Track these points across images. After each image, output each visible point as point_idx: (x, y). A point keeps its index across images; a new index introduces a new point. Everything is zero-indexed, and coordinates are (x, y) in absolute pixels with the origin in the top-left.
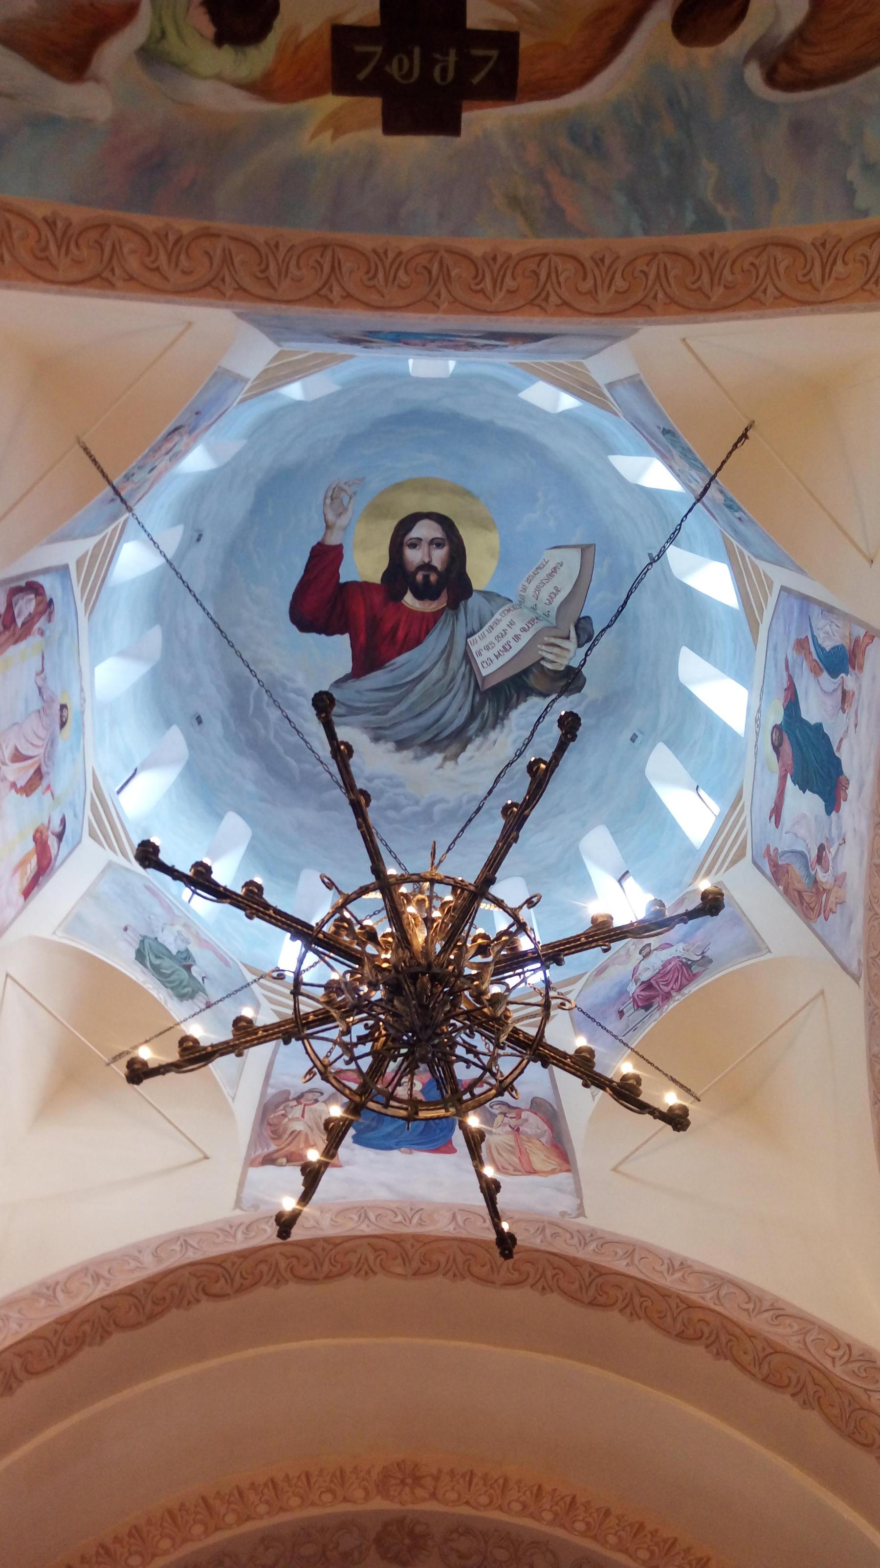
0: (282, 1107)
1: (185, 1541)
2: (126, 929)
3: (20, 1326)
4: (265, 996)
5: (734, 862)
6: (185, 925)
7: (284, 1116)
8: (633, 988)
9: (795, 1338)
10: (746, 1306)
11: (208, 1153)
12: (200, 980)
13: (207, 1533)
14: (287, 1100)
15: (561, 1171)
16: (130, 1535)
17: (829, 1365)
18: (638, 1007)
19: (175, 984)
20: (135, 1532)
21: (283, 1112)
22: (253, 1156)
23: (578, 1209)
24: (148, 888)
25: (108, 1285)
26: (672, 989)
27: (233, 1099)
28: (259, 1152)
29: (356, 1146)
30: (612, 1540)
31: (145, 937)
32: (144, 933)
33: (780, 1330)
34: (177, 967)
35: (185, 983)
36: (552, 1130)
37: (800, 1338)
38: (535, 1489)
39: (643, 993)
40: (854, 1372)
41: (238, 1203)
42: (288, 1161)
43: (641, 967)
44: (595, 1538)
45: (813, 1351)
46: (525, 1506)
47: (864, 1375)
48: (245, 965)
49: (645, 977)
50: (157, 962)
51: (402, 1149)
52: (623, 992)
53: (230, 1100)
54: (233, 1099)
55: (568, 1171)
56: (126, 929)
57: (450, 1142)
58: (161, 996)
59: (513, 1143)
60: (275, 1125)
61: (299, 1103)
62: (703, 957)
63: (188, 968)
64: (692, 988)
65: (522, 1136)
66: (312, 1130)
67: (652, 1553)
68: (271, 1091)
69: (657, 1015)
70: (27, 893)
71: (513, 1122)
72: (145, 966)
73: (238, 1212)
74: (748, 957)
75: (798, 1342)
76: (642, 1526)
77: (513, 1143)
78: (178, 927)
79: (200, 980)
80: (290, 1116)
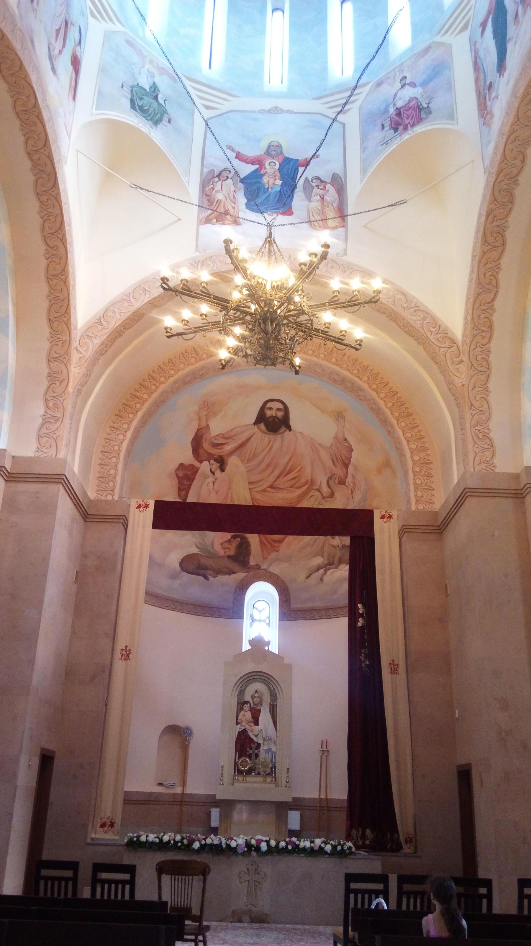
0: (211, 183)
1: (189, 365)
2: (122, 87)
3: (120, 315)
4: (198, 96)
5: (461, 31)
6: (151, 62)
7: (213, 188)
8: (392, 110)
9: (419, 322)
10: (404, 305)
11: (181, 218)
12: (163, 104)
13: (196, 362)
14: (214, 177)
15: (340, 227)
16: (169, 362)
17: (429, 335)
18: (392, 127)
19: (152, 115)
20: (170, 361)
21: (212, 186)
22: (201, 217)
23: (345, 251)
24: (127, 42)
25: (150, 294)
26: (409, 123)
27: (188, 183)
28: (203, 215)
29: (247, 211)
30: (345, 366)
31: (132, 87)
32: (131, 85)
33: (414, 318)
34: (151, 100)
35: (156, 112)
36: (339, 197)
37: (421, 322)
38: (318, 345)
39: (395, 117)
40: (438, 339)
41: (197, 250)
42: (217, 221)
43: (399, 95)
44: (338, 365)
45: (425, 329)
46: (314, 351)
47: (441, 340)
48: (185, 76)
49: (400, 104)
50: (140, 103)
51: (269, 212)
52: (386, 111)
53: (187, 184)
54: (188, 183)
55: (343, 226)
56: (122, 87)
57: (291, 207)
58: (147, 129)
59: (320, 208)
60: (209, 196)
61: (220, 179)
62: (428, 107)
63: (156, 98)
64: (419, 129)
65: (325, 203)
66: (226, 200)
67: (358, 371)
68: (206, 170)
69: (398, 140)
70: (74, 98)
71: (321, 192)
72: (136, 110)
73: (197, 254)
74: (448, 122)
75: (420, 324)
76: (356, 360)
77: (320, 208)
78: (148, 66)
79: (163, 104)
80: (216, 189)
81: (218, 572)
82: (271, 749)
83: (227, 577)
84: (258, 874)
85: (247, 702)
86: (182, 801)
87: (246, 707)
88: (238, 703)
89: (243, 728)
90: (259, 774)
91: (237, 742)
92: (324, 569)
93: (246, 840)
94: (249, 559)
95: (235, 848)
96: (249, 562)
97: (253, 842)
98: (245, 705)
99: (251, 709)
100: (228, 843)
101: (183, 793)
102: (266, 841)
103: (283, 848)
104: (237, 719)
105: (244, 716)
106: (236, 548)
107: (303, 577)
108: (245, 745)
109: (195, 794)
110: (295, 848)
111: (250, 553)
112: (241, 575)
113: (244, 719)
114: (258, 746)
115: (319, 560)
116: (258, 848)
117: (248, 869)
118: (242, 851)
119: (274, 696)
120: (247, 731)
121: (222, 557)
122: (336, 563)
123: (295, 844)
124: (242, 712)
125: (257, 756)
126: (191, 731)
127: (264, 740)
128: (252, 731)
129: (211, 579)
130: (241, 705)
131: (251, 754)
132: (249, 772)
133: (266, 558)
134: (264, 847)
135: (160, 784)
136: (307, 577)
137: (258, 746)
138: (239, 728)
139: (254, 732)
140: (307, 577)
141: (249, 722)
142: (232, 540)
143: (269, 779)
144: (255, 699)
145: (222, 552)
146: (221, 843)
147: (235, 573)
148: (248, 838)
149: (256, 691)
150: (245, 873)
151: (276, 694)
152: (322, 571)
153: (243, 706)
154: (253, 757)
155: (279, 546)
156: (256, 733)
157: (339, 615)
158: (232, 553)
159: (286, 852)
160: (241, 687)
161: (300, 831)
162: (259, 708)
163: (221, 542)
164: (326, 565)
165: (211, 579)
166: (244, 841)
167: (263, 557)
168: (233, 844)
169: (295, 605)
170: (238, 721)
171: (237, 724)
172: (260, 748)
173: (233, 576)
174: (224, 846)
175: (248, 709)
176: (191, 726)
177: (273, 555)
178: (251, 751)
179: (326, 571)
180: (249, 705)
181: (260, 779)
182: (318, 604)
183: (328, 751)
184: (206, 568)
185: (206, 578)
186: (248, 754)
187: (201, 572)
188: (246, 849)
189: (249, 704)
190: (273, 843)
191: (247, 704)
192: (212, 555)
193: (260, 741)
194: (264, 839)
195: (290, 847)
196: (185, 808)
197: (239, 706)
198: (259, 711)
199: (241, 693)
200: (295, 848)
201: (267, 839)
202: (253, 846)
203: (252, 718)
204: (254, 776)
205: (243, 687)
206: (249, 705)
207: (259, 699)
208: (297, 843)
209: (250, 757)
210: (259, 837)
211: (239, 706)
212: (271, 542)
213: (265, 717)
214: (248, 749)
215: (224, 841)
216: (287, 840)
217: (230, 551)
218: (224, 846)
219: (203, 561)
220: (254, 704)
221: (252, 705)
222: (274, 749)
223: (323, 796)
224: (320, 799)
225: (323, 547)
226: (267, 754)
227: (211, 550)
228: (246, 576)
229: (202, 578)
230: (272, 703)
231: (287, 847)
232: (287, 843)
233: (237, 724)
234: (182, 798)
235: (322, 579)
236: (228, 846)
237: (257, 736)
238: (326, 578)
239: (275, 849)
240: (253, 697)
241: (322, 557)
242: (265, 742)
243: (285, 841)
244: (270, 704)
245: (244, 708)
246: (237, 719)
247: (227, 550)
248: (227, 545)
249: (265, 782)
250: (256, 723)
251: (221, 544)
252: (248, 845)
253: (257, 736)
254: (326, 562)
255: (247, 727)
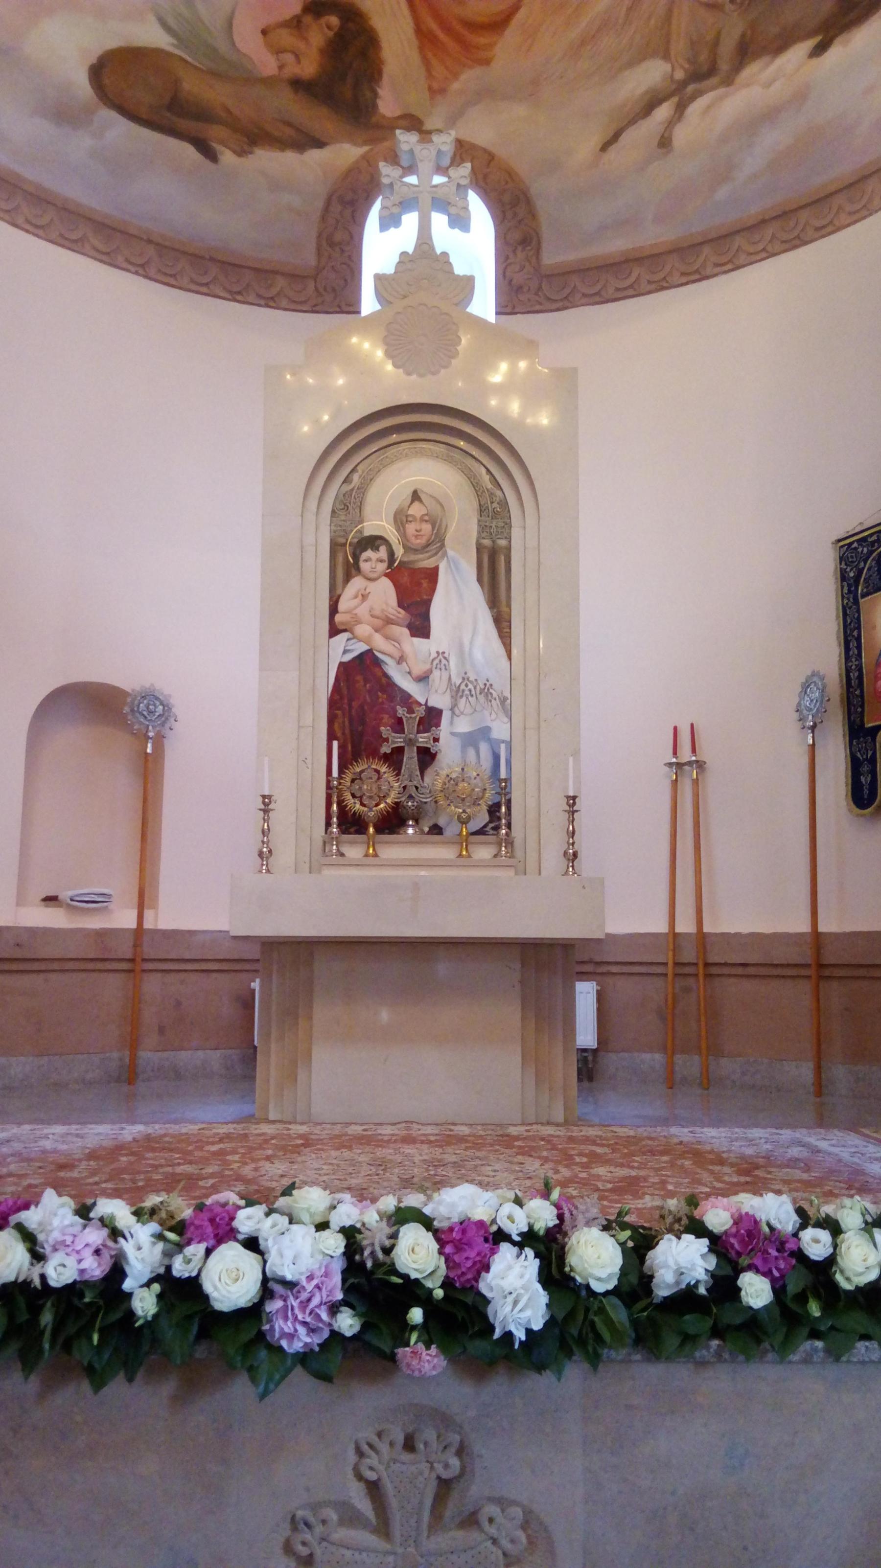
81: (253, 137)
82: (488, 729)
83: (290, 157)
84: (471, 1521)
85: (374, 542)
86: (139, 957)
87: (373, 561)
88: (335, 547)
89: (361, 648)
90: (437, 830)
91: (334, 704)
92: (675, 99)
93: (350, 1233)
94: (376, 95)
95: (252, 1313)
96: (375, 106)
97: (418, 1255)
98: (369, 553)
99: (396, 572)
100: (180, 1268)
101: (139, 931)
102: (529, 1238)
103: (685, 1299)
104: (334, 610)
105: (364, 597)
106: (322, 51)
107: (585, 147)
108: (368, 718)
109: (192, 933)
110: (802, 1298)
111: (380, 73)
112: (345, 153)
113: (363, 611)
114: (431, 718)
115: (653, 73)
116: (459, 1315)
117: (374, 1488)
118: (316, 1340)
119: (494, 515)
120: (377, 663)
121: (268, 82)
122: (724, 66)
123: (800, 1256)
124: (357, 583)
125: (427, 757)
126: (167, 707)
127: (457, 693)
128: (401, 660)
129: (227, 157)
130: (348, 555)
131: (400, 751)
132: (392, 822)
133: (442, 91)
134: (515, 1292)
135: (51, 900)
136: (605, 147)
137: (431, 718)
138: (342, 649)
139: (408, 662)
140: (605, 147)
141: (389, 621)
142: (308, 19)
143: (483, 852)
144: (411, 528)
145: (267, 64)
146: (117, 1272)
147: (320, 144)
148: (371, 1218)
149: (416, 496)
150: (350, 1517)
151: (504, 504)
152: (663, 112)
153: (356, 558)
154: (410, 759)
155: (491, 46)
156: (418, 670)
157: (742, 259)
158: (309, 68)
159: (716, 1332)
160: (347, 480)
161: (595, 1052)
162: (428, 563)
163: (261, 26)
164: (684, 83)
165: (227, 157)
166: (335, 1243)
167: (430, 88)
168: (230, 1281)
169: (554, 256)
170: (338, 618)
171: (334, 631)
172: (438, 725)
173: (314, 155)
174: (145, 1304)
175: (382, 567)
176: (165, 686)
177: (469, 78)
178: (398, 740)
179: (681, 109)
180: (383, 552)
181: (446, 853)
182: (652, 235)
183: (700, 765)
184: (203, 114)
185: (210, 154)
186: (385, 749)
187: (183, 124)
188: (347, 1323)
189: (383, 549)
190: (597, 1258)
191: (376, 549)
192: (232, 72)
193: (439, 700)
194: (515, 1220)
195: (756, 1291)
196: (152, 985)
197: (340, 559)
198: (432, 575)
199: (350, 505)
200: (802, 1298)
201: (542, 1214)
202: (412, 1290)
203: (400, 605)
204: (411, 842)
205: (356, 477)
206: (383, 552)
207: (427, 528)
208: (816, 1244)
209: (394, 759)
210: (463, 1201)
211: (340, 559)
212: (458, 28)
213: (457, 601)
214: (385, 731)
215: (142, 1251)
216: (718, 1218)
217: (297, 57)
218: (145, 1304)
219: (192, 86)
220: (407, 549)
221: (399, 552)
222: (500, 730)
223: (685, 926)
224: (675, 936)
225: (668, 18)
226: (471, 752)
227: (223, 47)
228: (364, 157)
229: (189, 151)
230: (487, 542)
231: (725, 1286)
232: (717, 1243)
233: (334, 631)
234: (135, 946)
235: (665, 142)
236: (182, 1293)
237: (423, 679)
238: (681, 135)
239: (619, 1313)
240: (401, 519)
241: (666, 57)
242: (462, 702)
243: (698, 1229)
244: (480, 549)
245: (364, 566)
246: (334, 610)
247: (289, 58)
248: (286, 38)
249: (464, 859)
250: (420, 627)
251: (264, 32)
252: (370, 1282)
253: (423, 679)
254: (679, 75)
255: (379, 643)
